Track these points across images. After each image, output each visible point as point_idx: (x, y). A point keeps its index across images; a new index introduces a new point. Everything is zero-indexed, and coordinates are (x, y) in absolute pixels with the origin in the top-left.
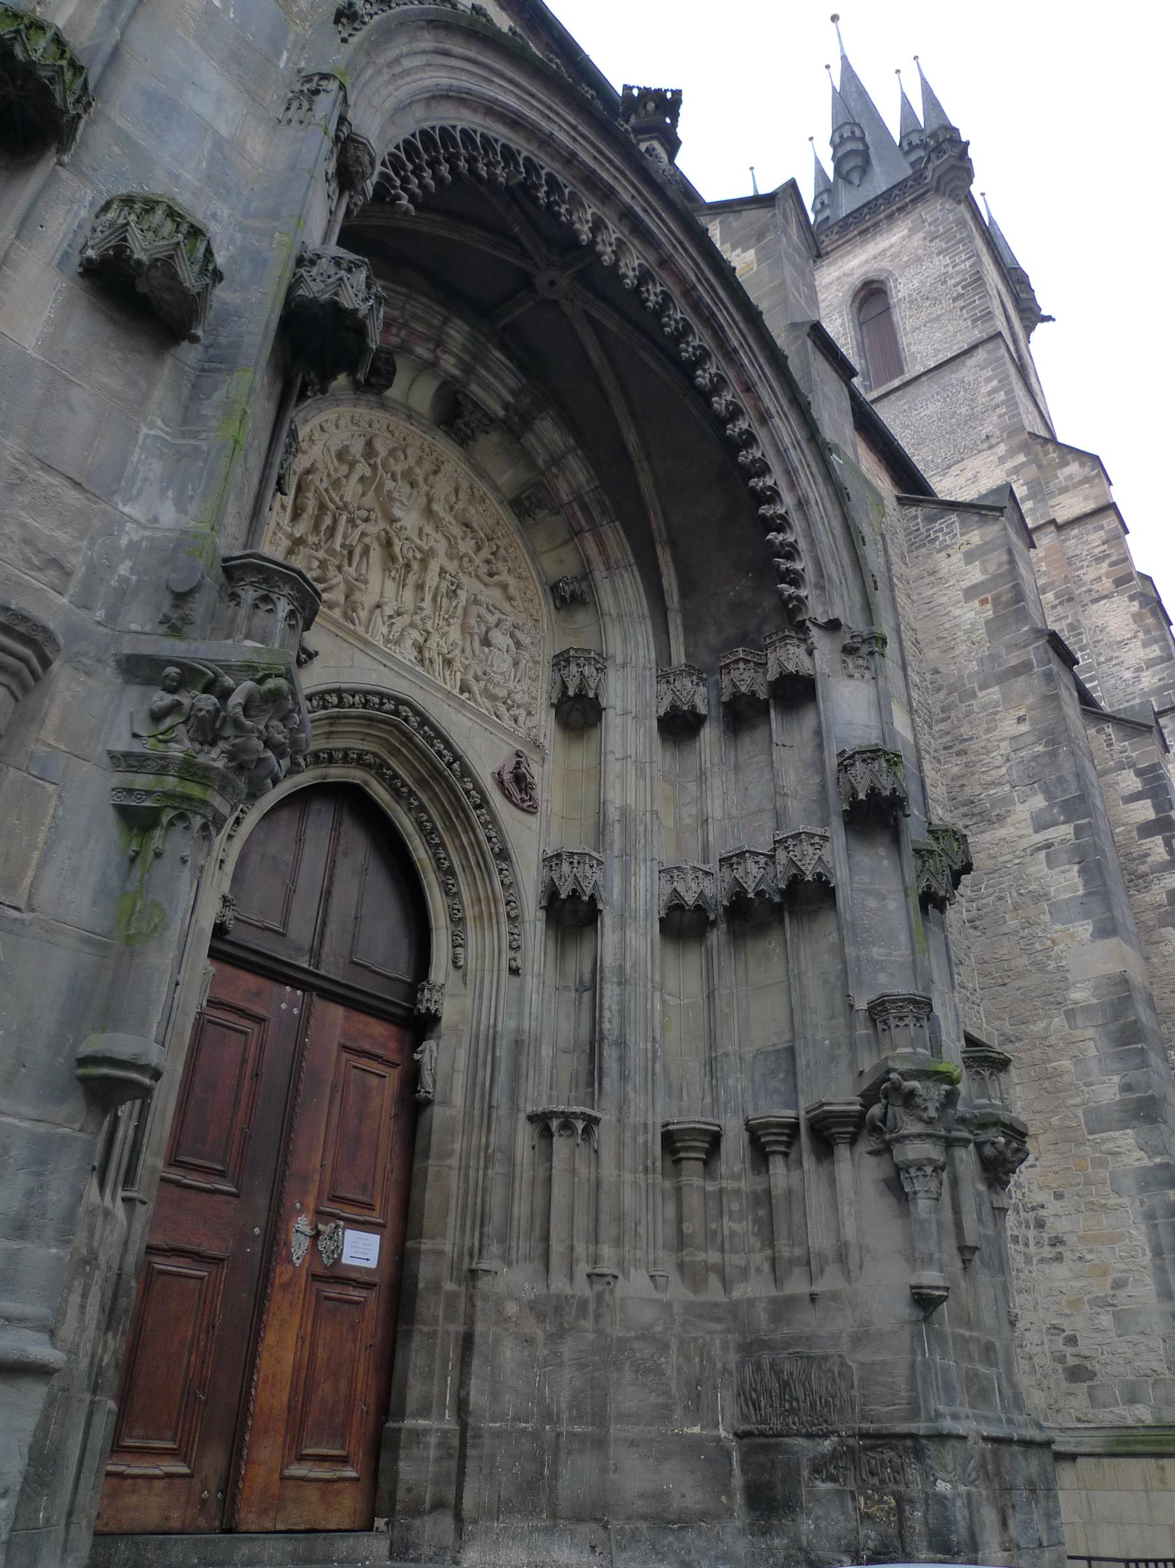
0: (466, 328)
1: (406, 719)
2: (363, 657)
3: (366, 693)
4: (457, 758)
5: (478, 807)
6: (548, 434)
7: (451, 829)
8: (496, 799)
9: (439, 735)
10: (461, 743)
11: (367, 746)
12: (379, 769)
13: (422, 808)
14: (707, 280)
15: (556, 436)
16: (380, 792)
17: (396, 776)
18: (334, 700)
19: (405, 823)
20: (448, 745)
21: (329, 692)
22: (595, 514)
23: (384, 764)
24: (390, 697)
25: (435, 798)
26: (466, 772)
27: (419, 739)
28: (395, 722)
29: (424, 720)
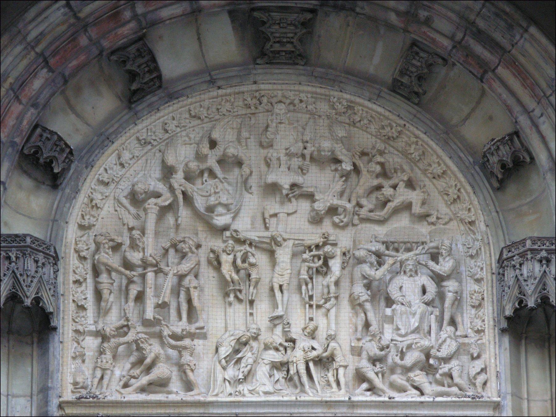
22: (497, 36)
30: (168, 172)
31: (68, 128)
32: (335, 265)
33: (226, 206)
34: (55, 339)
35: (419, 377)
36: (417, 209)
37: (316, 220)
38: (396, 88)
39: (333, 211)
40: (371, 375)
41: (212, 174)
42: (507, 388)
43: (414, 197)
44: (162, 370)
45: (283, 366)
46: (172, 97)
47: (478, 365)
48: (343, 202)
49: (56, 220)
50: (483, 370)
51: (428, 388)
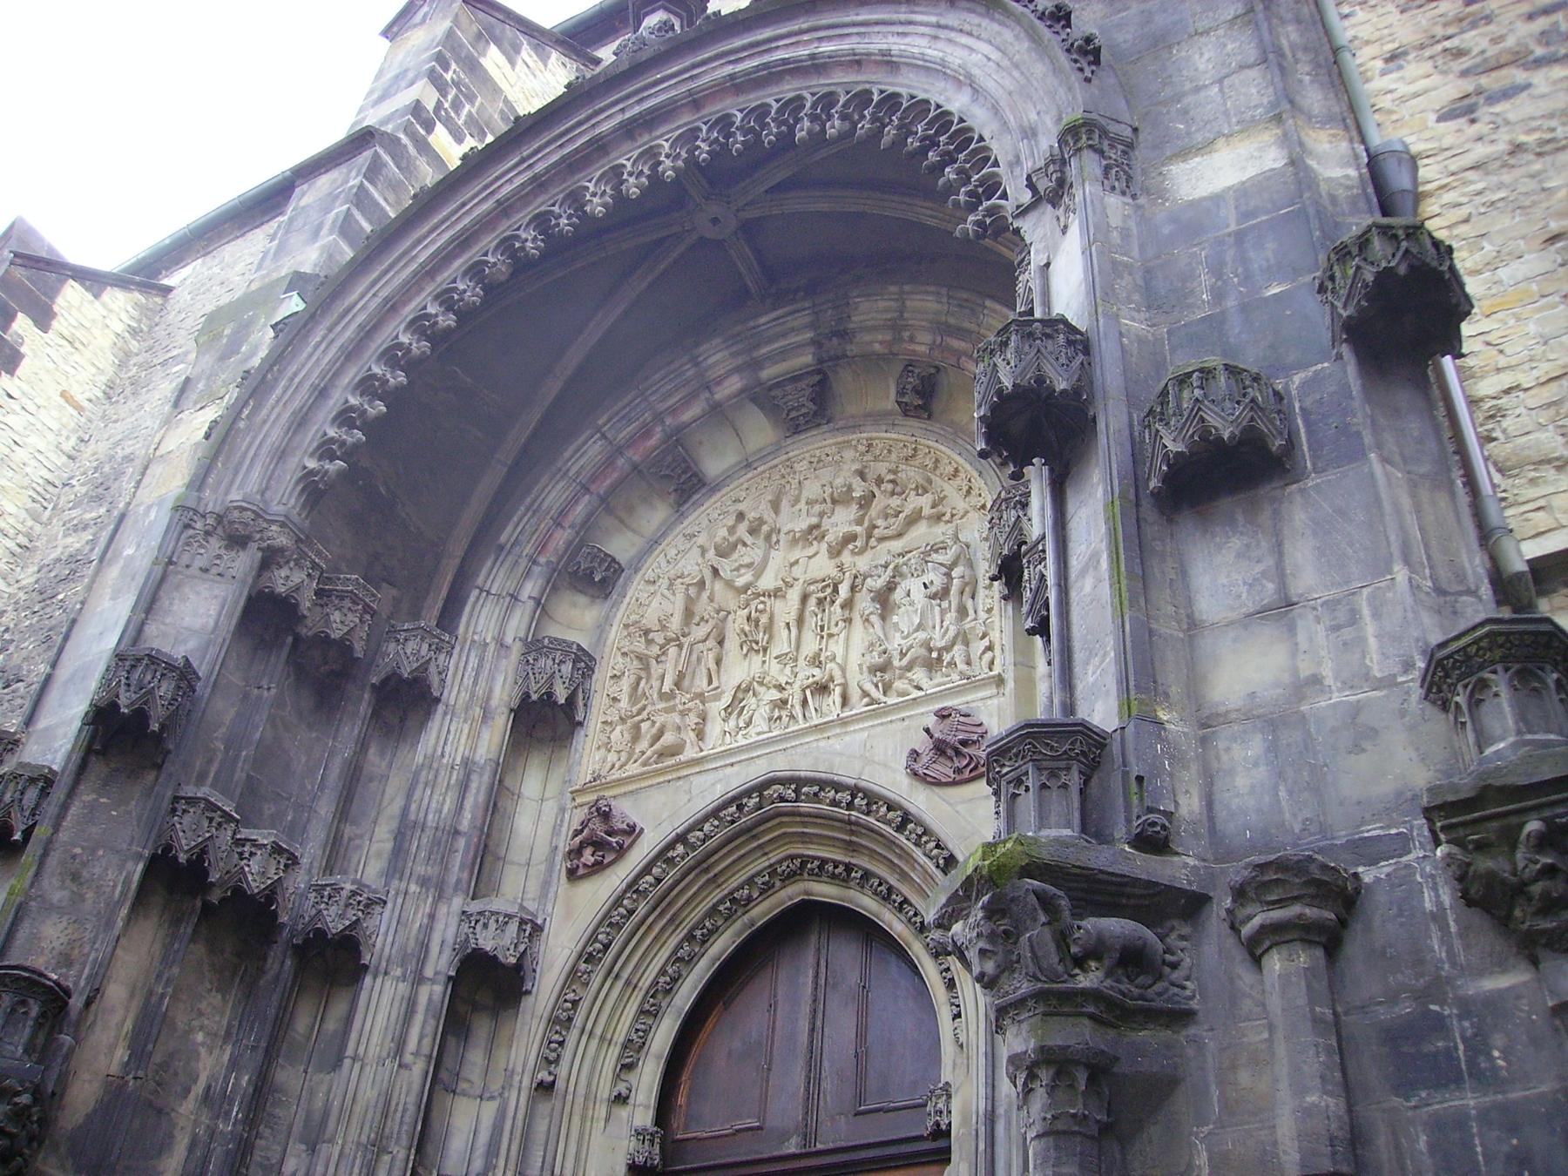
0: (717, 341)
1: (782, 799)
2: (704, 777)
3: (714, 813)
4: (855, 791)
5: (901, 828)
6: (871, 311)
7: (904, 876)
8: (921, 801)
9: (823, 784)
10: (847, 773)
11: (774, 857)
12: (801, 868)
13: (867, 875)
14: (744, 48)
15: (882, 304)
16: (825, 891)
17: (824, 861)
18: (680, 849)
19: (866, 903)
20: (838, 787)
21: (671, 846)
23: (805, 860)
24: (748, 793)
25: (873, 854)
26: (872, 798)
27: (805, 806)
28: (769, 813)
29: (798, 782)
30: (703, 551)
31: (620, 546)
32: (844, 590)
33: (749, 566)
34: (580, 735)
35: (919, 675)
36: (927, 511)
37: (835, 552)
38: (906, 410)
39: (851, 538)
40: (869, 687)
41: (745, 545)
42: (1010, 658)
43: (925, 502)
44: (669, 738)
45: (784, 702)
46: (714, 490)
47: (986, 642)
48: (858, 529)
49: (602, 628)
50: (990, 648)
51: (925, 683)
